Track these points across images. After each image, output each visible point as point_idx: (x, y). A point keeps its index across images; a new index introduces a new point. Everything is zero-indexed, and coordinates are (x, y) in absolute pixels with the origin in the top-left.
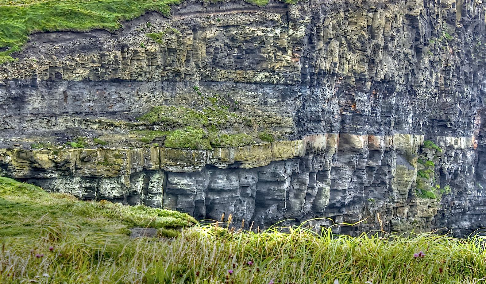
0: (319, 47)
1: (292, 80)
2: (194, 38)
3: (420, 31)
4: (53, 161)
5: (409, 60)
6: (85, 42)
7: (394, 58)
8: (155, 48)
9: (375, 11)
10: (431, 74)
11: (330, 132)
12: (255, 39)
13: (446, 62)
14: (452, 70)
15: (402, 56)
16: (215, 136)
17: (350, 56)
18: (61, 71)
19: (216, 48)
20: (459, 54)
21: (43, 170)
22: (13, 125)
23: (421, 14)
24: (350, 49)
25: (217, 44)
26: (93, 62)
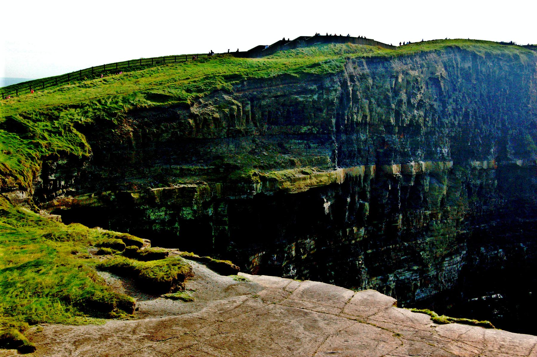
3: (443, 89)
14: (471, 114)
19: (269, 112)
20: (475, 102)
21: (137, 204)
24: (379, 105)
25: (270, 109)
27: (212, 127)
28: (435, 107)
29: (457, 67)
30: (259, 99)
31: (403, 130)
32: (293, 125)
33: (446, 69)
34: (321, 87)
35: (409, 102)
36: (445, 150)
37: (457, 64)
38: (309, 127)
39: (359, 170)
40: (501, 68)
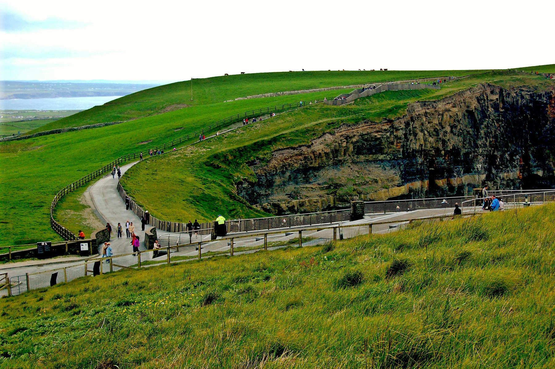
0: (410, 139)
1: (398, 157)
2: (347, 143)
4: (287, 206)
5: (470, 134)
6: (296, 152)
7: (458, 136)
8: (328, 150)
9: (442, 115)
10: (486, 140)
11: (422, 180)
12: (377, 139)
13: (495, 132)
15: (465, 133)
16: (360, 189)
17: (431, 139)
18: (287, 166)
19: (358, 146)
20: (503, 127)
22: (270, 192)
23: (475, 109)
24: (430, 136)
25: (358, 144)
26: (301, 160)
27: (324, 158)
28: (471, 133)
29: (487, 99)
30: (351, 138)
31: (447, 152)
32: (374, 154)
33: (479, 102)
34: (392, 127)
35: (452, 132)
36: (479, 166)
37: (487, 97)
38: (384, 155)
39: (417, 184)
40: (522, 97)
